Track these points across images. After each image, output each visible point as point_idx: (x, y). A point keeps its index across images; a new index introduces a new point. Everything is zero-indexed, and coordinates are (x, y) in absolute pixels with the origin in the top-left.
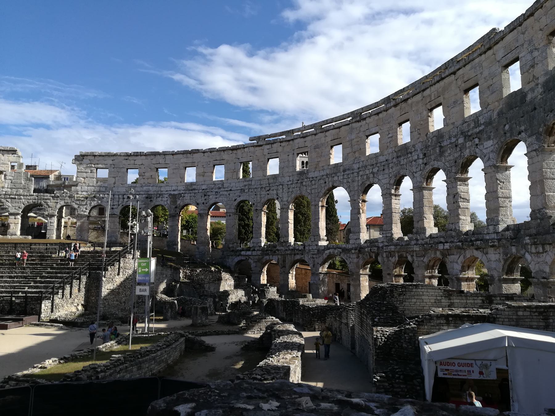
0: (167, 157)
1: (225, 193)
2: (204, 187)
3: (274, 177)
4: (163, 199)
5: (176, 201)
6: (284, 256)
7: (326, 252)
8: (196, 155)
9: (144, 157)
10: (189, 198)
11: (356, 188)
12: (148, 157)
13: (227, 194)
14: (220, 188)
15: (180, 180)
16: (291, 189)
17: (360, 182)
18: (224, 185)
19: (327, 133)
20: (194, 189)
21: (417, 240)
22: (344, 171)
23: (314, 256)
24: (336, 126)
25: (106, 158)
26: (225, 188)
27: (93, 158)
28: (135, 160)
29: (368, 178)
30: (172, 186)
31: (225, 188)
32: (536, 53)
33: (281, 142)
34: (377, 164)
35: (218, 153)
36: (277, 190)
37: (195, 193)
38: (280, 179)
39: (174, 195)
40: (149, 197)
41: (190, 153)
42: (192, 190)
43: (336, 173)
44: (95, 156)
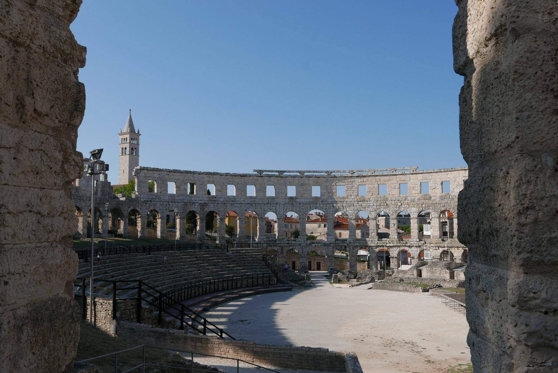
0: (195, 175)
2: (222, 200)
3: (272, 198)
4: (195, 206)
6: (282, 248)
7: (312, 245)
8: (215, 176)
9: (179, 174)
10: (213, 207)
11: (332, 212)
18: (236, 199)
22: (322, 201)
23: (303, 247)
24: (317, 176)
25: (155, 172)
26: (236, 201)
27: (146, 171)
28: (173, 176)
31: (236, 201)
32: (436, 185)
35: (231, 177)
41: (211, 175)
44: (148, 170)
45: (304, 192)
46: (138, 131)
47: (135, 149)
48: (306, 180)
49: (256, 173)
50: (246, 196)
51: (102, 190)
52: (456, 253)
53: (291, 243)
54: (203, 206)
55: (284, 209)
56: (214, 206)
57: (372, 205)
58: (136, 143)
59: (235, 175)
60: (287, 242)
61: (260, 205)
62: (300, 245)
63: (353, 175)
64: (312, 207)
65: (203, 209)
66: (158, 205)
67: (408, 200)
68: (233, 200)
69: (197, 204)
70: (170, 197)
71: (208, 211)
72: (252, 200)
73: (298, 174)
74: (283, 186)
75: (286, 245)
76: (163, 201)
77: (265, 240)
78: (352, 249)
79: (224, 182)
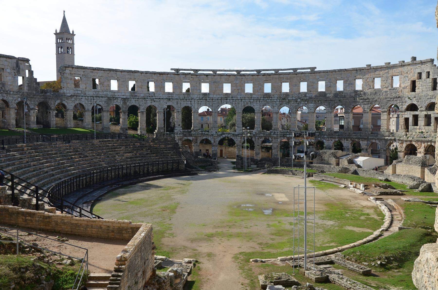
0: (118, 73)
2: (142, 95)
4: (118, 101)
5: (126, 103)
7: (223, 136)
8: (136, 74)
9: (102, 72)
10: (134, 101)
11: (240, 107)
12: (106, 72)
14: (152, 96)
15: (126, 89)
17: (242, 105)
19: (222, 77)
20: (136, 96)
21: (275, 132)
22: (232, 98)
23: (215, 137)
24: (228, 75)
25: (80, 70)
27: (71, 69)
28: (97, 73)
32: (332, 84)
34: (251, 98)
42: (134, 96)
45: (216, 89)
46: (73, 32)
47: (71, 48)
48: (218, 78)
49: (173, 71)
50: (165, 92)
51: (28, 86)
52: (345, 144)
53: (204, 134)
54: (125, 100)
55: (198, 104)
56: (135, 100)
57: (276, 100)
58: (71, 43)
59: (154, 73)
60: (200, 133)
61: (177, 100)
62: (212, 135)
63: (259, 74)
64: (223, 102)
65: (125, 103)
66: (83, 100)
67: (307, 97)
68: (153, 95)
69: (120, 99)
71: (130, 105)
72: (170, 95)
73: (211, 72)
74: (198, 84)
75: (200, 135)
76: (88, 95)
77: (182, 131)
78: (257, 140)
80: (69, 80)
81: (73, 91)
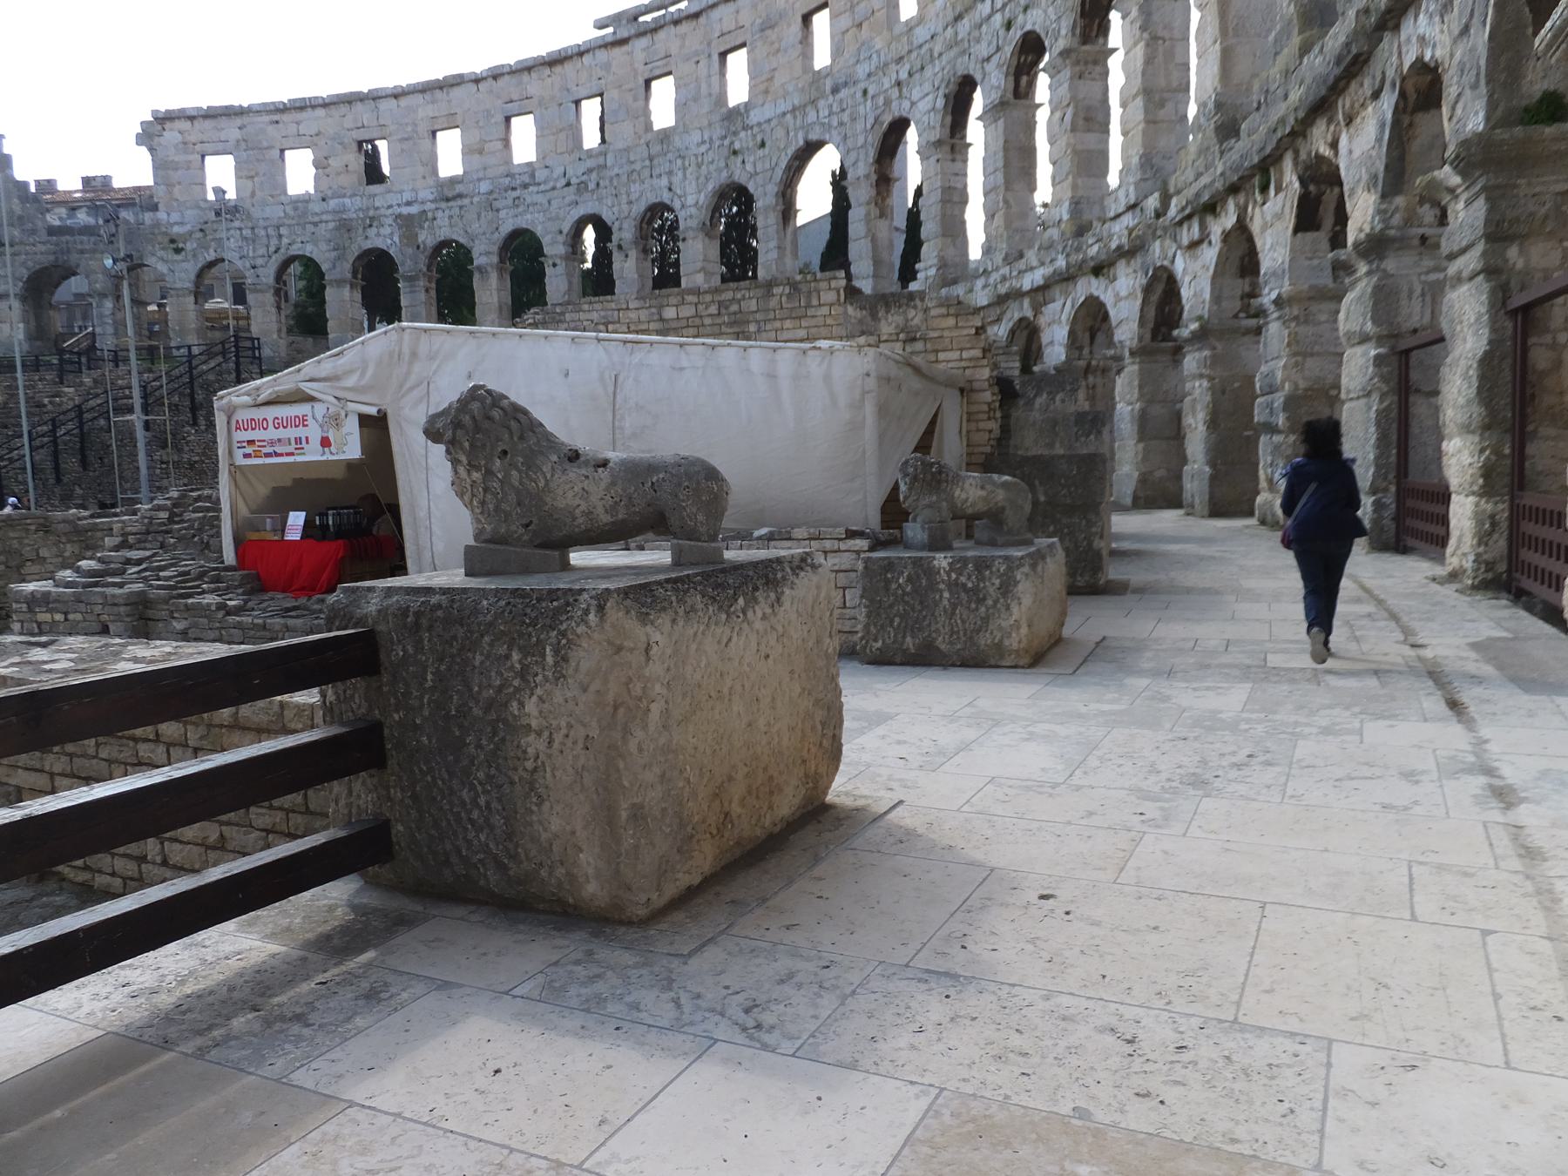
1: (541, 199)
2: (484, 187)
4: (382, 231)
8: (457, 93)
9: (320, 112)
11: (861, 140)
12: (335, 112)
13: (545, 202)
14: (525, 186)
16: (704, 167)
17: (871, 121)
20: (460, 196)
22: (835, 90)
25: (223, 122)
26: (539, 184)
27: (186, 125)
29: (888, 102)
30: (401, 192)
31: (539, 184)
33: (676, 22)
34: (910, 52)
35: (513, 80)
36: (670, 173)
37: (461, 207)
38: (677, 141)
39: (410, 217)
40: (345, 227)
43: (813, 102)
44: (192, 118)
56: (451, 217)
59: (528, 68)
66: (232, 243)
68: (526, 179)
70: (289, 209)
79: (488, 111)
80: (177, 169)
81: (195, 212)
